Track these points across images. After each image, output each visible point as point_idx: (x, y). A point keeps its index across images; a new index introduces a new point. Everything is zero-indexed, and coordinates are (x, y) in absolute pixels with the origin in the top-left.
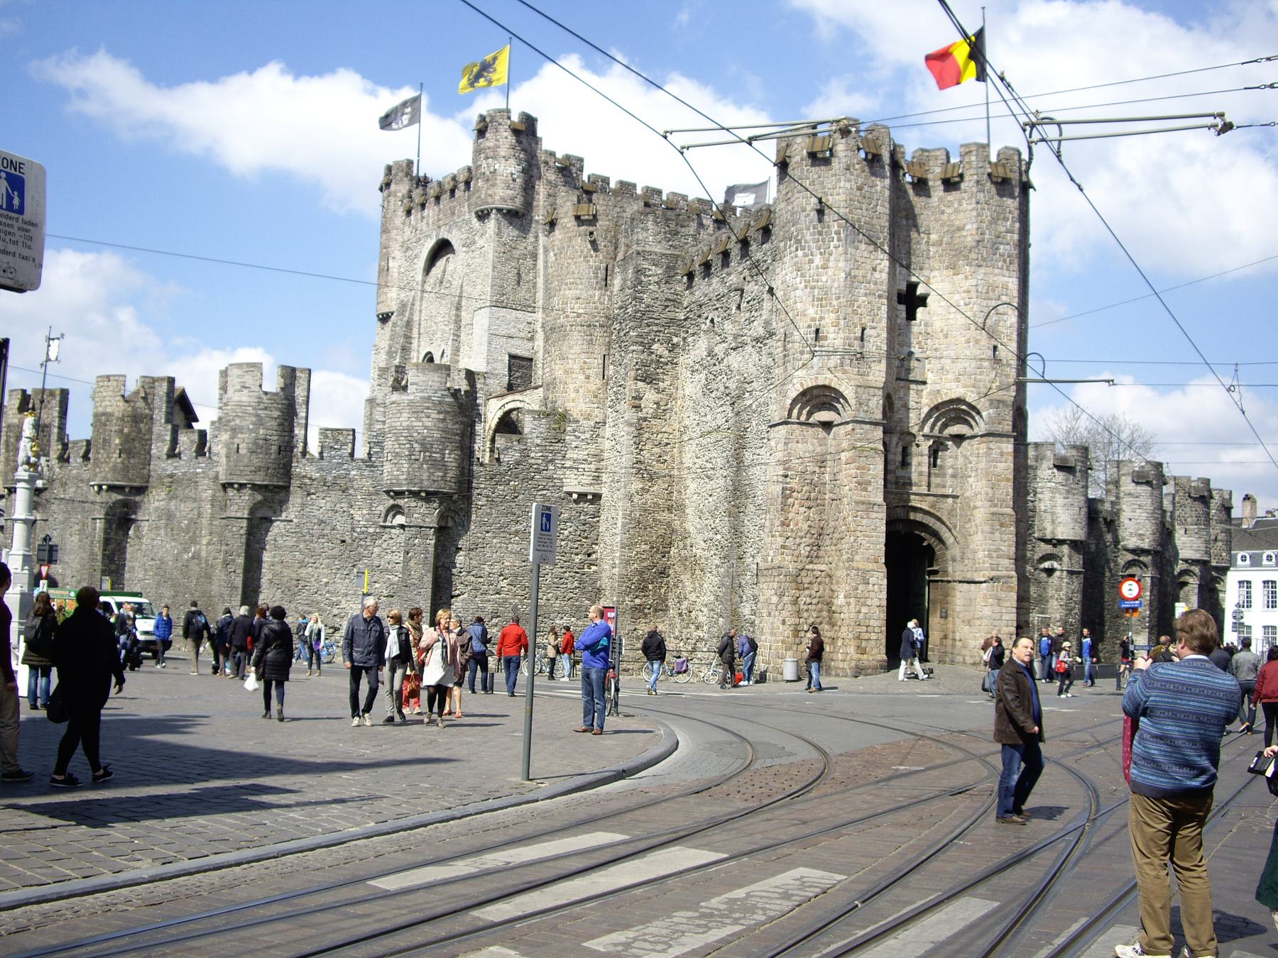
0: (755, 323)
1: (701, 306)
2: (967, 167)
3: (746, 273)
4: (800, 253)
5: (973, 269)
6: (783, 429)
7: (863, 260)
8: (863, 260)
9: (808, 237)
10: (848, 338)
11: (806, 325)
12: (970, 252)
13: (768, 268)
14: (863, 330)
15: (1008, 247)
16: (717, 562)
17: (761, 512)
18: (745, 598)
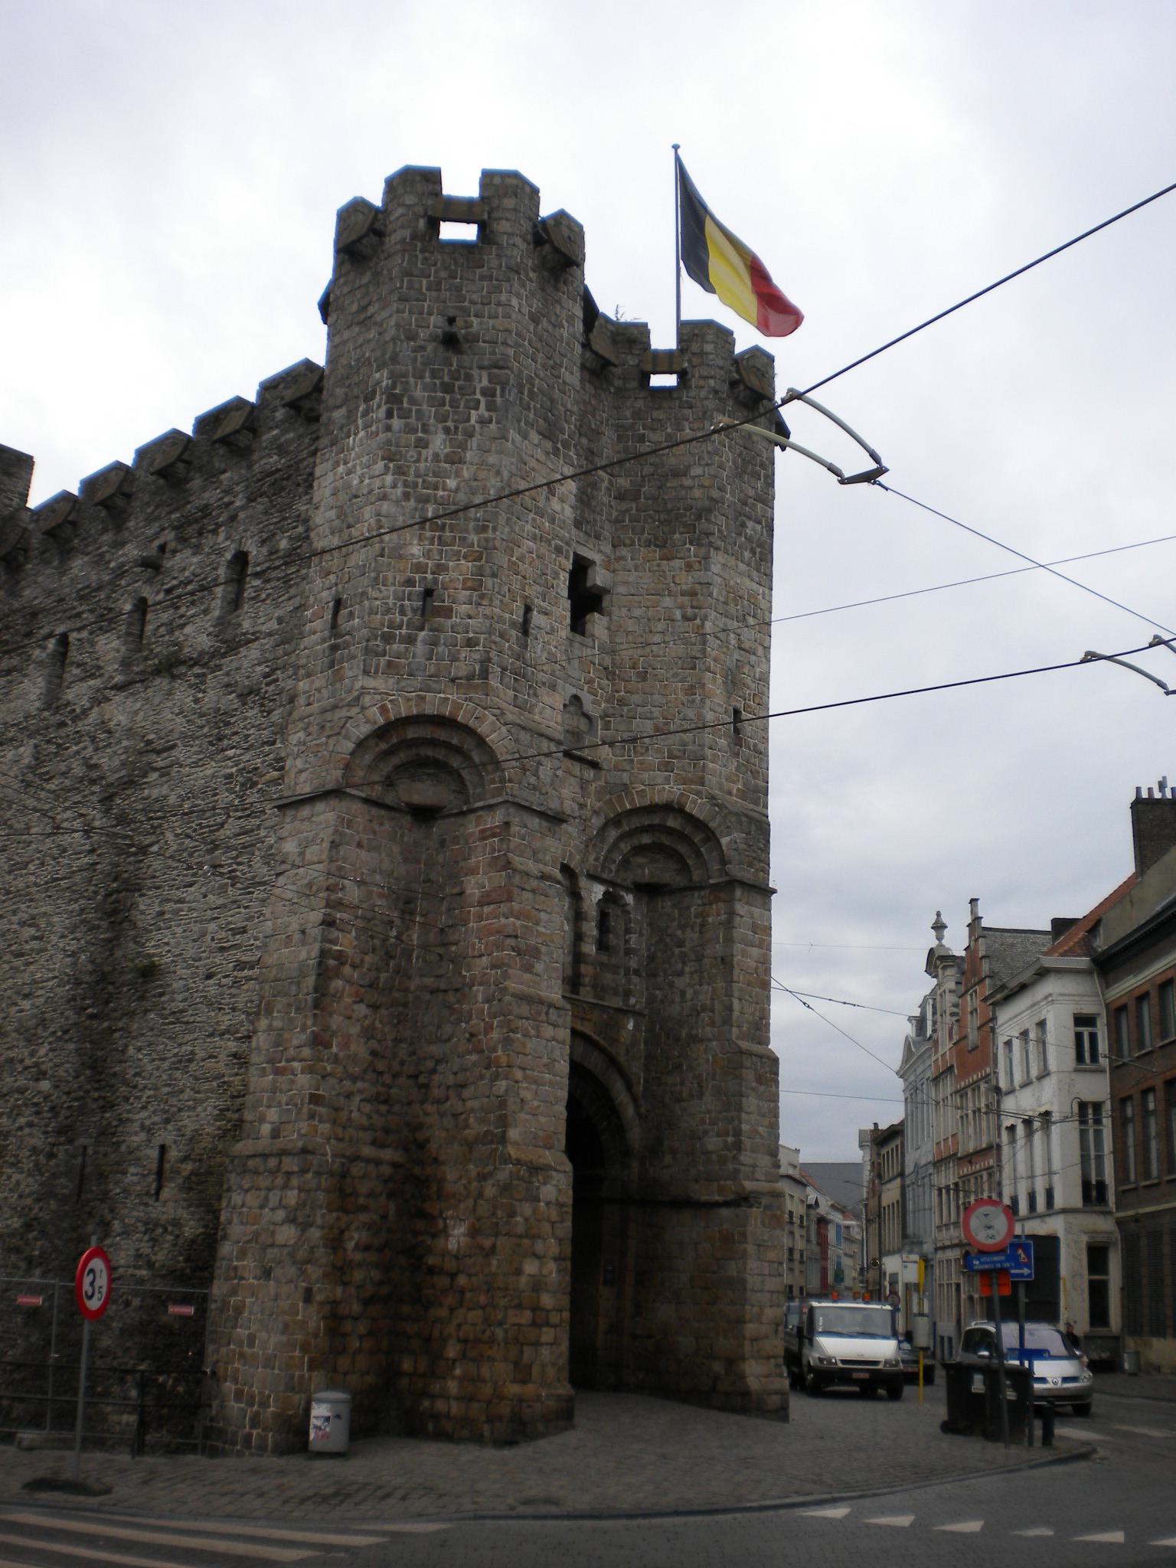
0: (188, 630)
1: (34, 615)
2: (695, 361)
3: (169, 536)
4: (396, 423)
5: (703, 551)
6: (326, 815)
7: (533, 463)
8: (533, 463)
9: (419, 393)
10: (501, 620)
11: (400, 578)
12: (699, 517)
13: (233, 518)
14: (528, 609)
15: (758, 527)
16: (37, 1140)
17: (178, 1028)
18: (117, 1226)
